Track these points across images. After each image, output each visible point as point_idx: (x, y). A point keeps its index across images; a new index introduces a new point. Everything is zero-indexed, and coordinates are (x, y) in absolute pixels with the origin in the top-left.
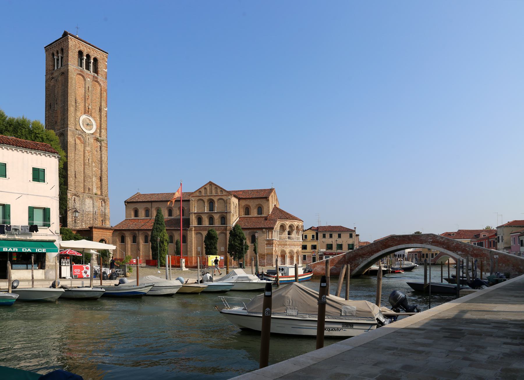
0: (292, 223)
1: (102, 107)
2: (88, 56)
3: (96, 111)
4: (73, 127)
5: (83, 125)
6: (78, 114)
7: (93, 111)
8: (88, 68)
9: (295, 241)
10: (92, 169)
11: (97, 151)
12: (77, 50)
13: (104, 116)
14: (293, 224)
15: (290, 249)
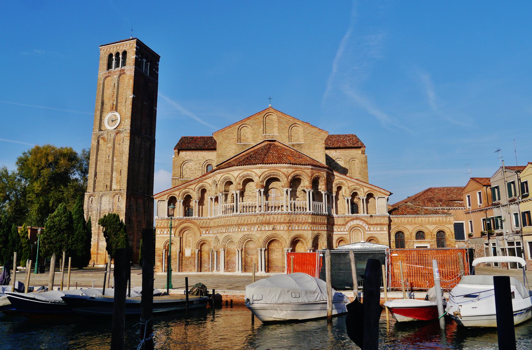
0: (228, 175)
1: (128, 96)
2: (118, 54)
3: (122, 104)
4: (97, 130)
5: (108, 123)
6: (104, 114)
7: (119, 105)
8: (117, 66)
9: (235, 216)
10: (112, 164)
11: (119, 144)
12: (107, 55)
13: (129, 104)
14: (231, 176)
15: (226, 234)
